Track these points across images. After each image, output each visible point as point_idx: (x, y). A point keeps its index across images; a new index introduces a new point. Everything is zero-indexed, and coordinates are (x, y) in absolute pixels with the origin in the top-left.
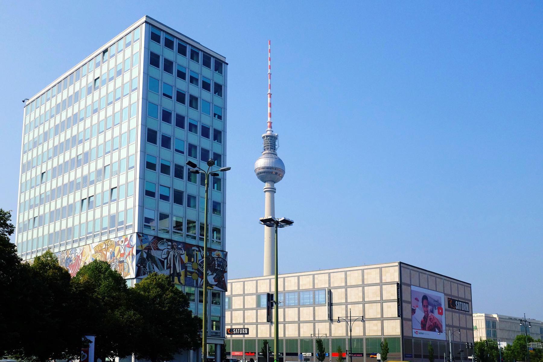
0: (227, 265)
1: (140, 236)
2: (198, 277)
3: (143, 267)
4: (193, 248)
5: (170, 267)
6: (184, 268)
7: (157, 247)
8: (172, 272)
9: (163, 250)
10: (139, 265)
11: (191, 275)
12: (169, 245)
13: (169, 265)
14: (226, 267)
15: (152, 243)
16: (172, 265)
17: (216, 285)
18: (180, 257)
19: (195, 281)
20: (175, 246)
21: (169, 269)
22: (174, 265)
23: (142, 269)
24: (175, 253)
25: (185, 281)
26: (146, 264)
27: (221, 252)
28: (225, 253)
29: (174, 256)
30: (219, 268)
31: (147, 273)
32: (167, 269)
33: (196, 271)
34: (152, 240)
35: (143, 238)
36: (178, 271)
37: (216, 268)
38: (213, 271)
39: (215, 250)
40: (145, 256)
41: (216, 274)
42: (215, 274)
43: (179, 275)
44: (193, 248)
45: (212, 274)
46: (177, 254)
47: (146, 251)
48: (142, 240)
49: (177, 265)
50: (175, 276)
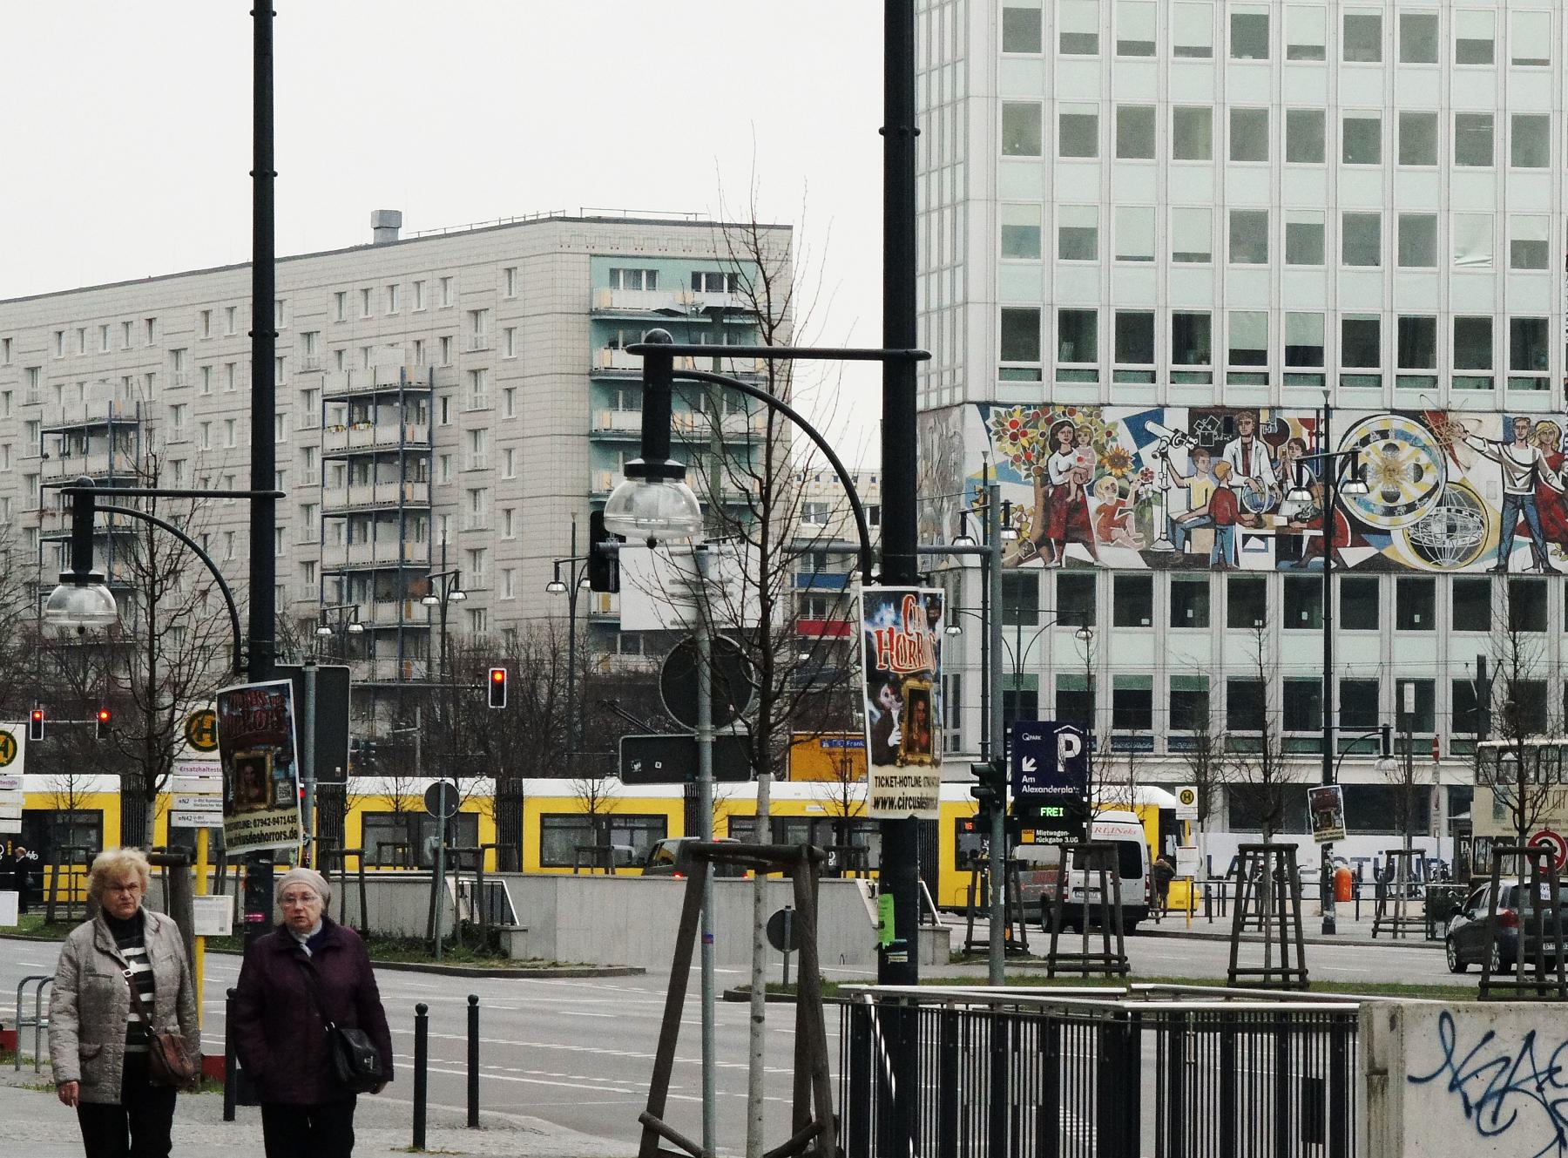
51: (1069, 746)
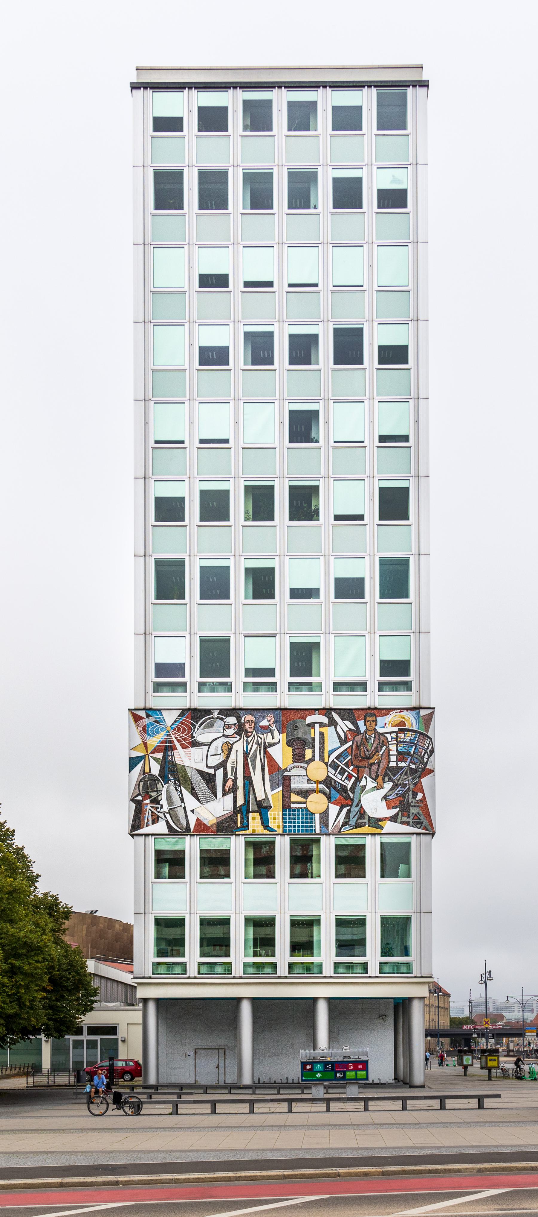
0: (433, 748)
1: (142, 718)
2: (329, 801)
4: (310, 719)
5: (234, 790)
6: (281, 782)
7: (193, 737)
8: (240, 801)
9: (209, 745)
10: (139, 798)
11: (304, 800)
12: (229, 726)
13: (230, 783)
14: (429, 757)
15: (175, 729)
16: (240, 783)
17: (394, 819)
18: (266, 752)
19: (317, 816)
20: (247, 726)
21: (232, 795)
22: (248, 779)
23: (149, 806)
24: (248, 743)
26: (159, 792)
27: (410, 711)
28: (423, 713)
29: (246, 754)
30: (403, 764)
31: (162, 815)
32: (225, 794)
33: (321, 786)
34: (175, 721)
35: (147, 721)
36: (260, 796)
37: (392, 764)
38: (380, 778)
39: (387, 711)
40: (155, 769)
41: (391, 784)
42: (388, 786)
43: (263, 808)
44: (310, 719)
45: (377, 788)
46: (255, 746)
47: (160, 755)
48: (145, 729)
49: (256, 778)
50: (252, 812)
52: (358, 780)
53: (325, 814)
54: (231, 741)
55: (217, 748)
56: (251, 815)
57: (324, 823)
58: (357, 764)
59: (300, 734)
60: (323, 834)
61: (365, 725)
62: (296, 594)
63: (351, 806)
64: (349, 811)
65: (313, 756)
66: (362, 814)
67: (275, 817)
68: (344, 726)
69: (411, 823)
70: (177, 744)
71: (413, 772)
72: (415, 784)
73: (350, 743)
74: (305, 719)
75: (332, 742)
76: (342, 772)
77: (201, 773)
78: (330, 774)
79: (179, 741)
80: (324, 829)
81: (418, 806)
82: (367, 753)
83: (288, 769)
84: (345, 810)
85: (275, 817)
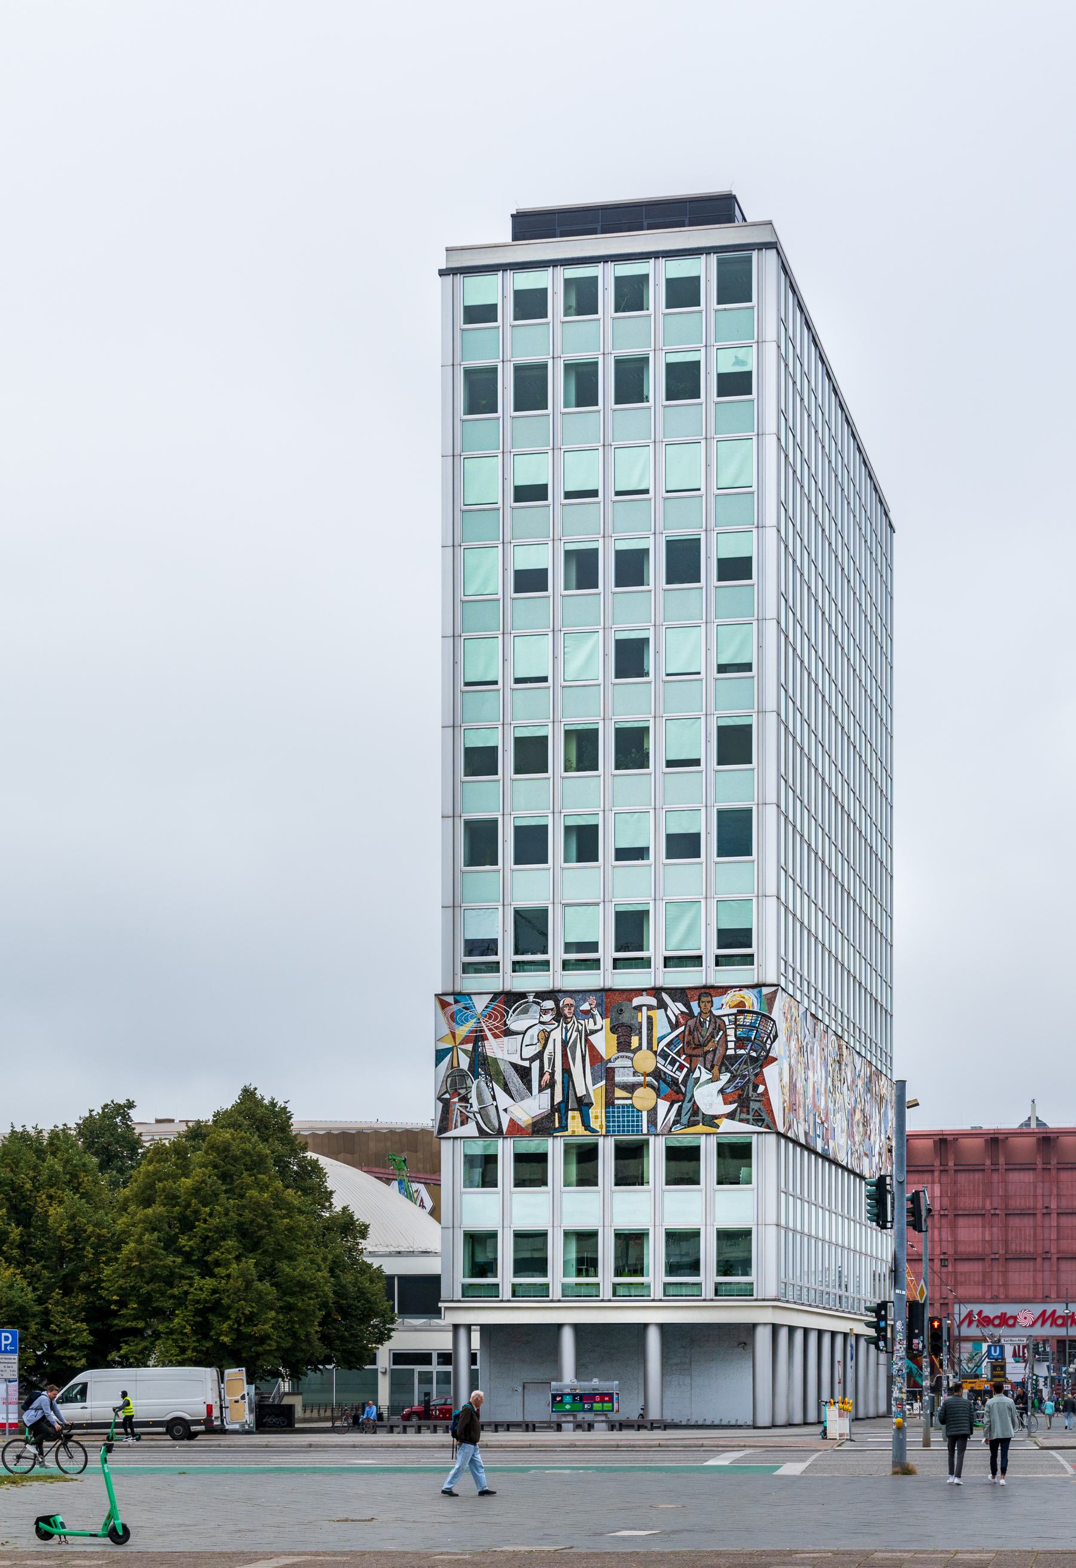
0: (776, 1032)
1: (449, 1004)
2: (658, 1096)
3: (460, 1100)
5: (551, 1085)
6: (604, 1075)
7: (506, 1025)
8: (558, 1098)
9: (524, 1033)
10: (447, 1096)
12: (545, 1012)
13: (547, 1077)
14: (772, 1043)
15: (486, 1016)
16: (558, 1077)
17: (731, 1116)
18: (587, 1040)
19: (645, 1114)
20: (566, 1011)
21: (549, 1091)
22: (567, 1071)
23: (457, 1106)
24: (567, 1031)
25: (608, 1121)
26: (468, 1089)
27: (750, 990)
29: (565, 1043)
30: (742, 1052)
31: (471, 1115)
32: (541, 1090)
33: (649, 1079)
34: (486, 1007)
35: (455, 1008)
36: (581, 1091)
37: (730, 1052)
38: (716, 1068)
39: (724, 990)
40: (464, 1063)
41: (729, 1075)
42: (725, 1077)
43: (583, 1105)
44: (636, 1001)
45: (712, 1080)
47: (469, 1047)
48: (453, 1017)
49: (576, 1070)
50: (571, 1110)
51: (7, 1338)
52: (691, 1071)
53: (653, 1112)
54: (548, 1028)
55: (533, 1036)
56: (570, 1113)
57: (652, 1121)
58: (690, 1052)
59: (625, 1018)
60: (651, 1135)
61: (699, 1006)
62: (623, 854)
63: (683, 1101)
64: (680, 1108)
65: (640, 1044)
66: (695, 1110)
67: (597, 1114)
68: (676, 1008)
69: (751, 1120)
70: (488, 1034)
71: (754, 1060)
72: (756, 1075)
73: (682, 1029)
74: (631, 1001)
75: (661, 1027)
76: (673, 1062)
77: (515, 1066)
78: (659, 1065)
79: (490, 1030)
80: (652, 1129)
81: (759, 1101)
82: (701, 1039)
83: (612, 1060)
84: (676, 1106)
85: (597, 1114)
